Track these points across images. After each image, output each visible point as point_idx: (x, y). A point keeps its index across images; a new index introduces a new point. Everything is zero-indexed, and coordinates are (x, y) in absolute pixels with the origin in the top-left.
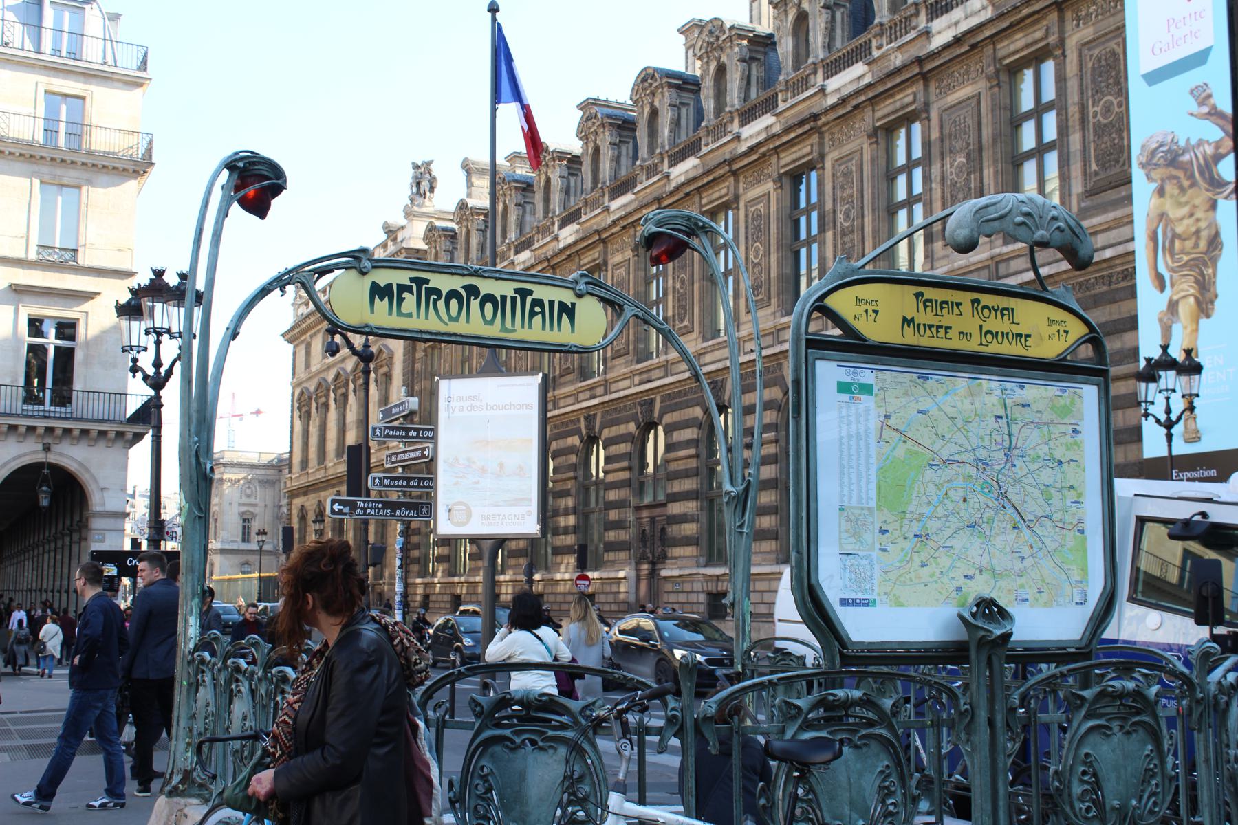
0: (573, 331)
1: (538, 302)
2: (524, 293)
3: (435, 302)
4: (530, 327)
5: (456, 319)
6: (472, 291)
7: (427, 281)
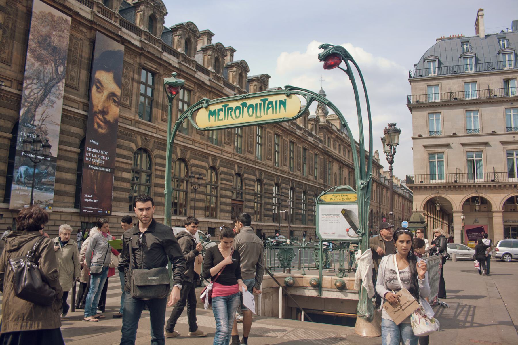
0: (285, 112)
1: (271, 103)
2: (264, 101)
3: (231, 112)
4: (267, 114)
5: (239, 117)
6: (244, 105)
7: (228, 105)
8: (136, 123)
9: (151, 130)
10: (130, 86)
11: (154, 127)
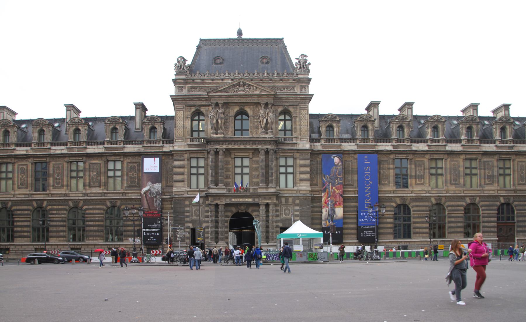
8: (394, 192)
9: (406, 192)
10: (387, 173)
11: (409, 191)
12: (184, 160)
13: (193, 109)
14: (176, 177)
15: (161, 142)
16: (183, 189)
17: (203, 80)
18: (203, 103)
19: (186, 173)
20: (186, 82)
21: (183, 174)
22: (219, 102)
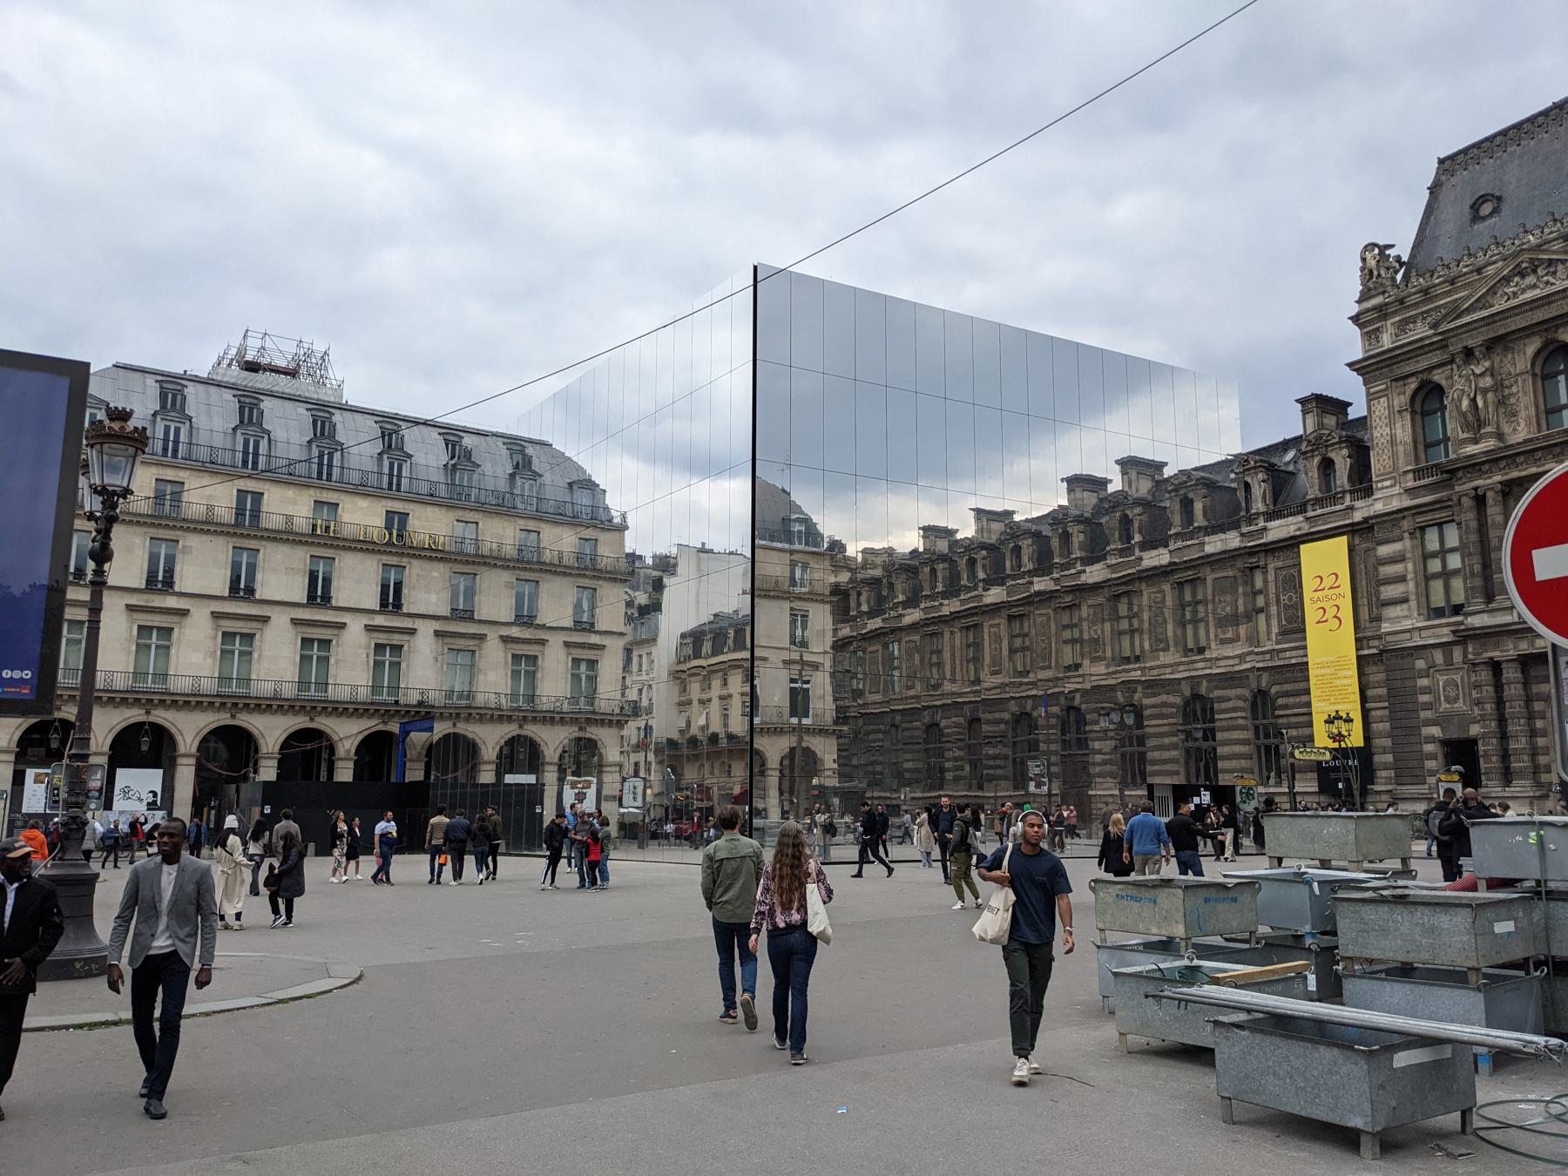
12: (1401, 539)
13: (1413, 384)
14: (1389, 592)
15: (1348, 496)
16: (1407, 624)
17: (1425, 291)
18: (1435, 358)
19: (1410, 576)
20: (1382, 312)
21: (1402, 579)
22: (1470, 343)
